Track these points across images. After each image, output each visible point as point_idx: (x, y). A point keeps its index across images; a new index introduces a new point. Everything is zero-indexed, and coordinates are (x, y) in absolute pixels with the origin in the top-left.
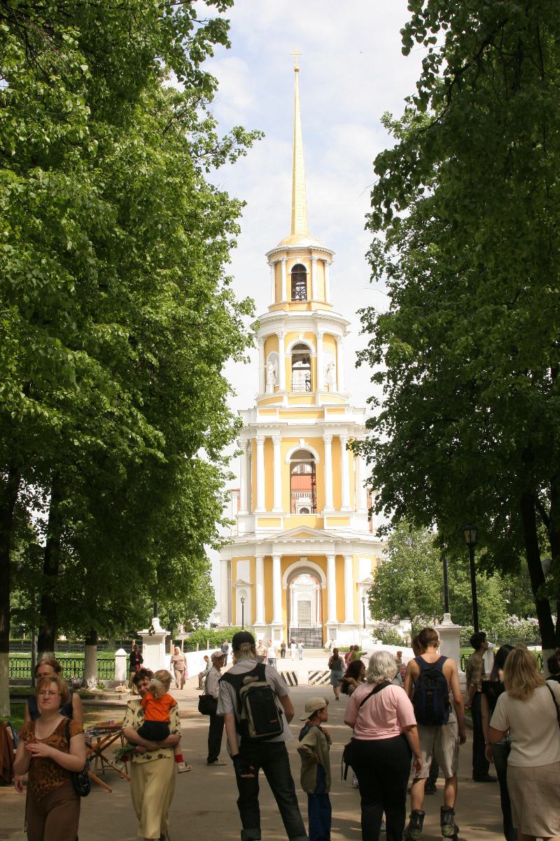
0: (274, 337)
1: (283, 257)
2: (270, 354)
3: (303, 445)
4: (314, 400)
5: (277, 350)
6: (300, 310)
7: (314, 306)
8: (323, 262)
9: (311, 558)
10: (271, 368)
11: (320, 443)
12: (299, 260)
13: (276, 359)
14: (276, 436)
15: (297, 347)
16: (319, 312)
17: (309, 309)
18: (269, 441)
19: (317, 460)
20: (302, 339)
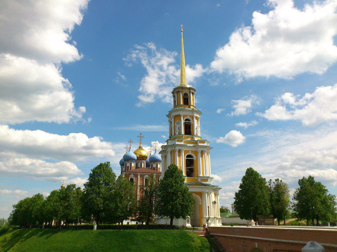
0: (179, 116)
1: (181, 90)
2: (176, 123)
3: (190, 153)
4: (192, 138)
5: (180, 120)
6: (187, 108)
7: (192, 107)
8: (193, 93)
9: (196, 193)
10: (178, 126)
11: (196, 153)
12: (186, 91)
13: (180, 123)
14: (184, 149)
15: (186, 120)
16: (194, 109)
17: (190, 108)
18: (180, 151)
19: (195, 158)
20: (188, 117)
